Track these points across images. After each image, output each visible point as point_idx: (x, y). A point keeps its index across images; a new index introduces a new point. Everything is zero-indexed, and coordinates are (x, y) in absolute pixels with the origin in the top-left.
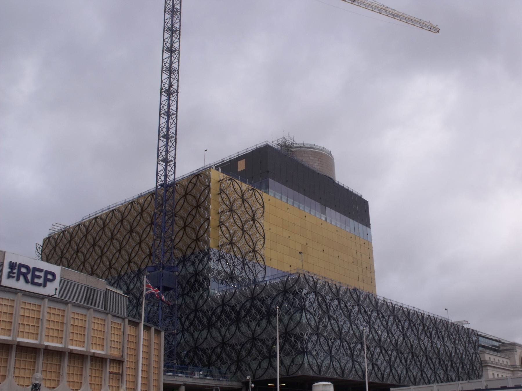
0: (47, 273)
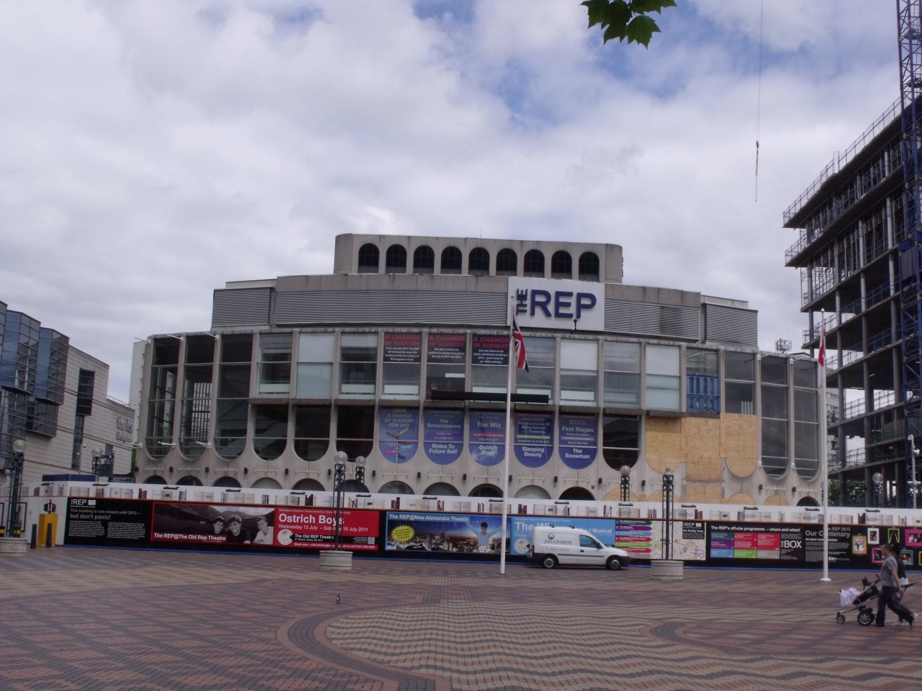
0: (580, 296)
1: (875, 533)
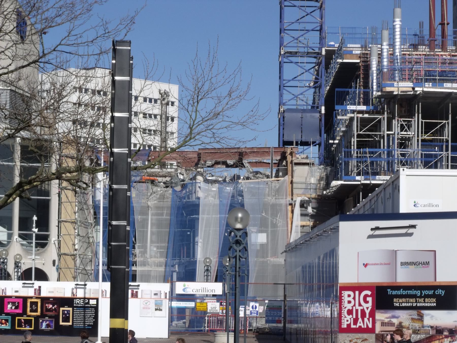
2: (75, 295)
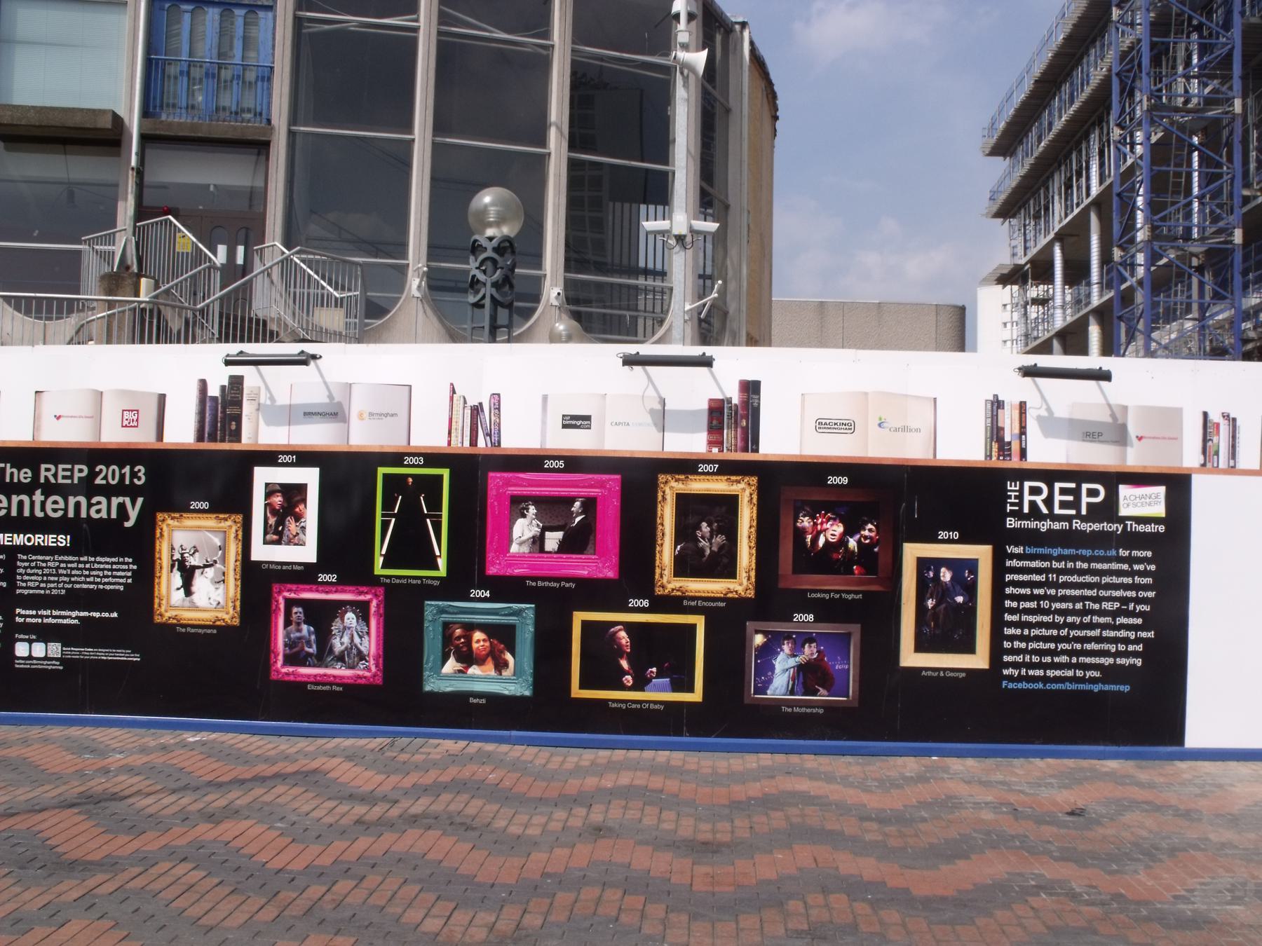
1: (294, 493)
2: (1015, 447)
